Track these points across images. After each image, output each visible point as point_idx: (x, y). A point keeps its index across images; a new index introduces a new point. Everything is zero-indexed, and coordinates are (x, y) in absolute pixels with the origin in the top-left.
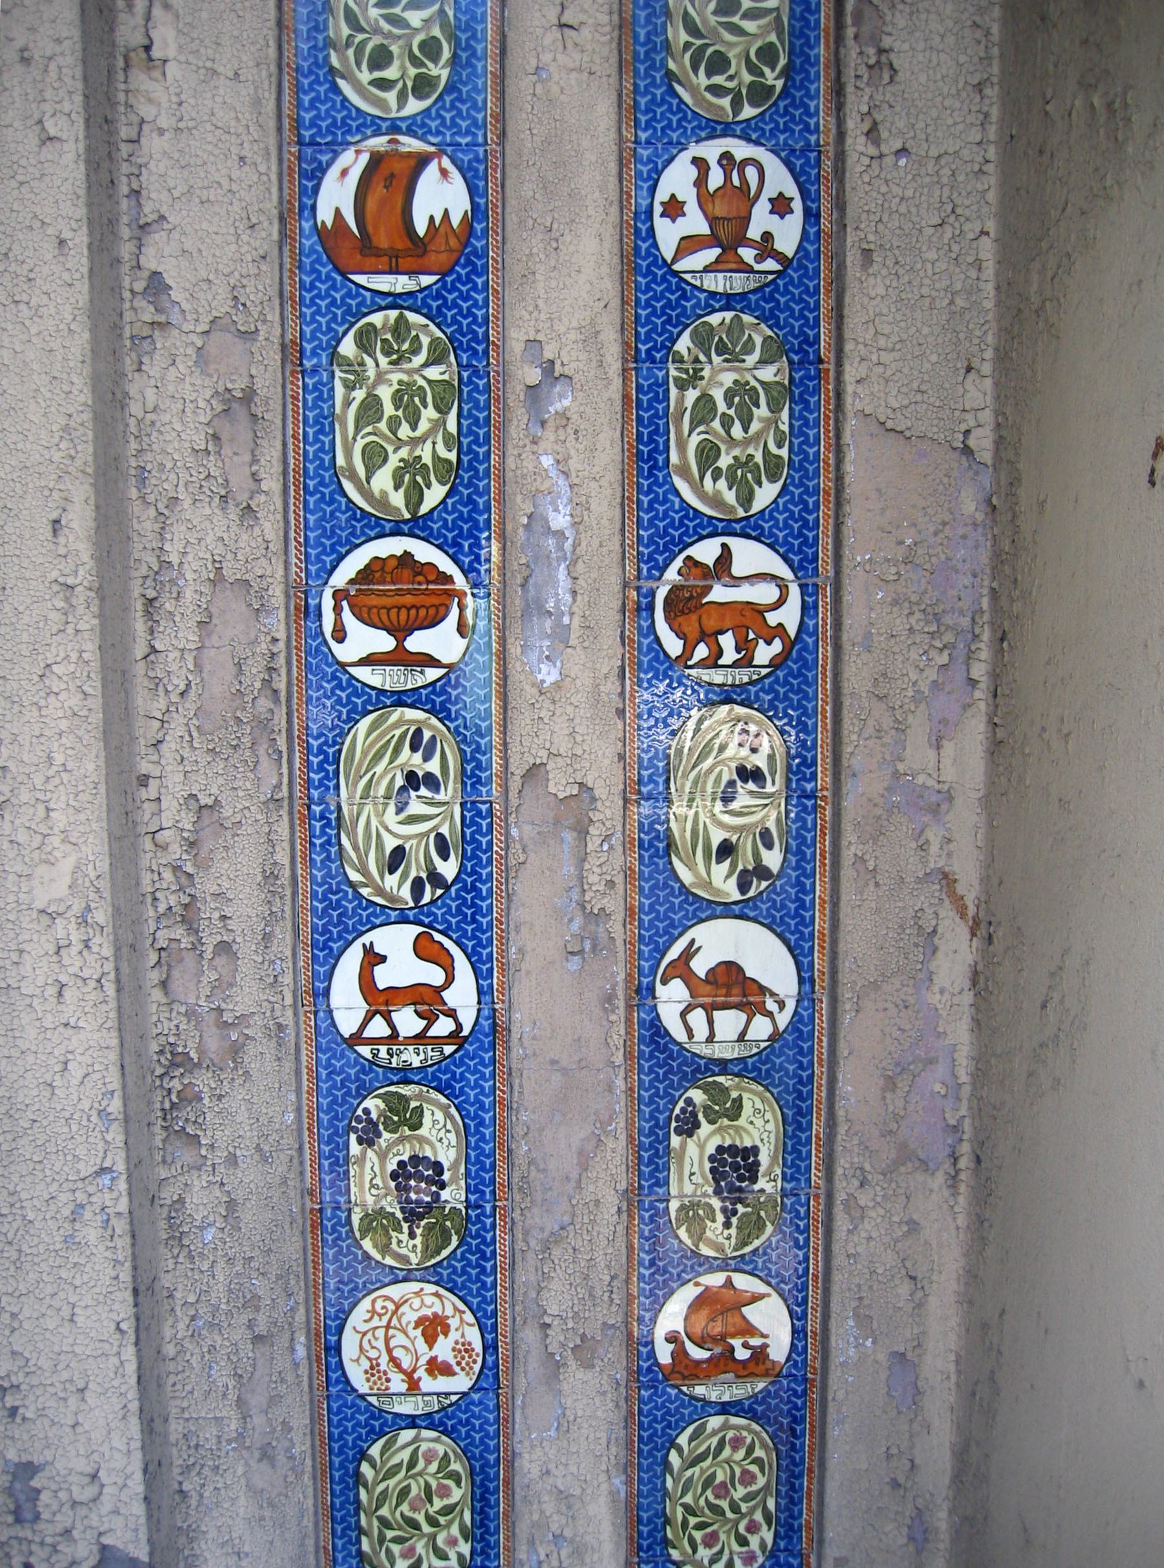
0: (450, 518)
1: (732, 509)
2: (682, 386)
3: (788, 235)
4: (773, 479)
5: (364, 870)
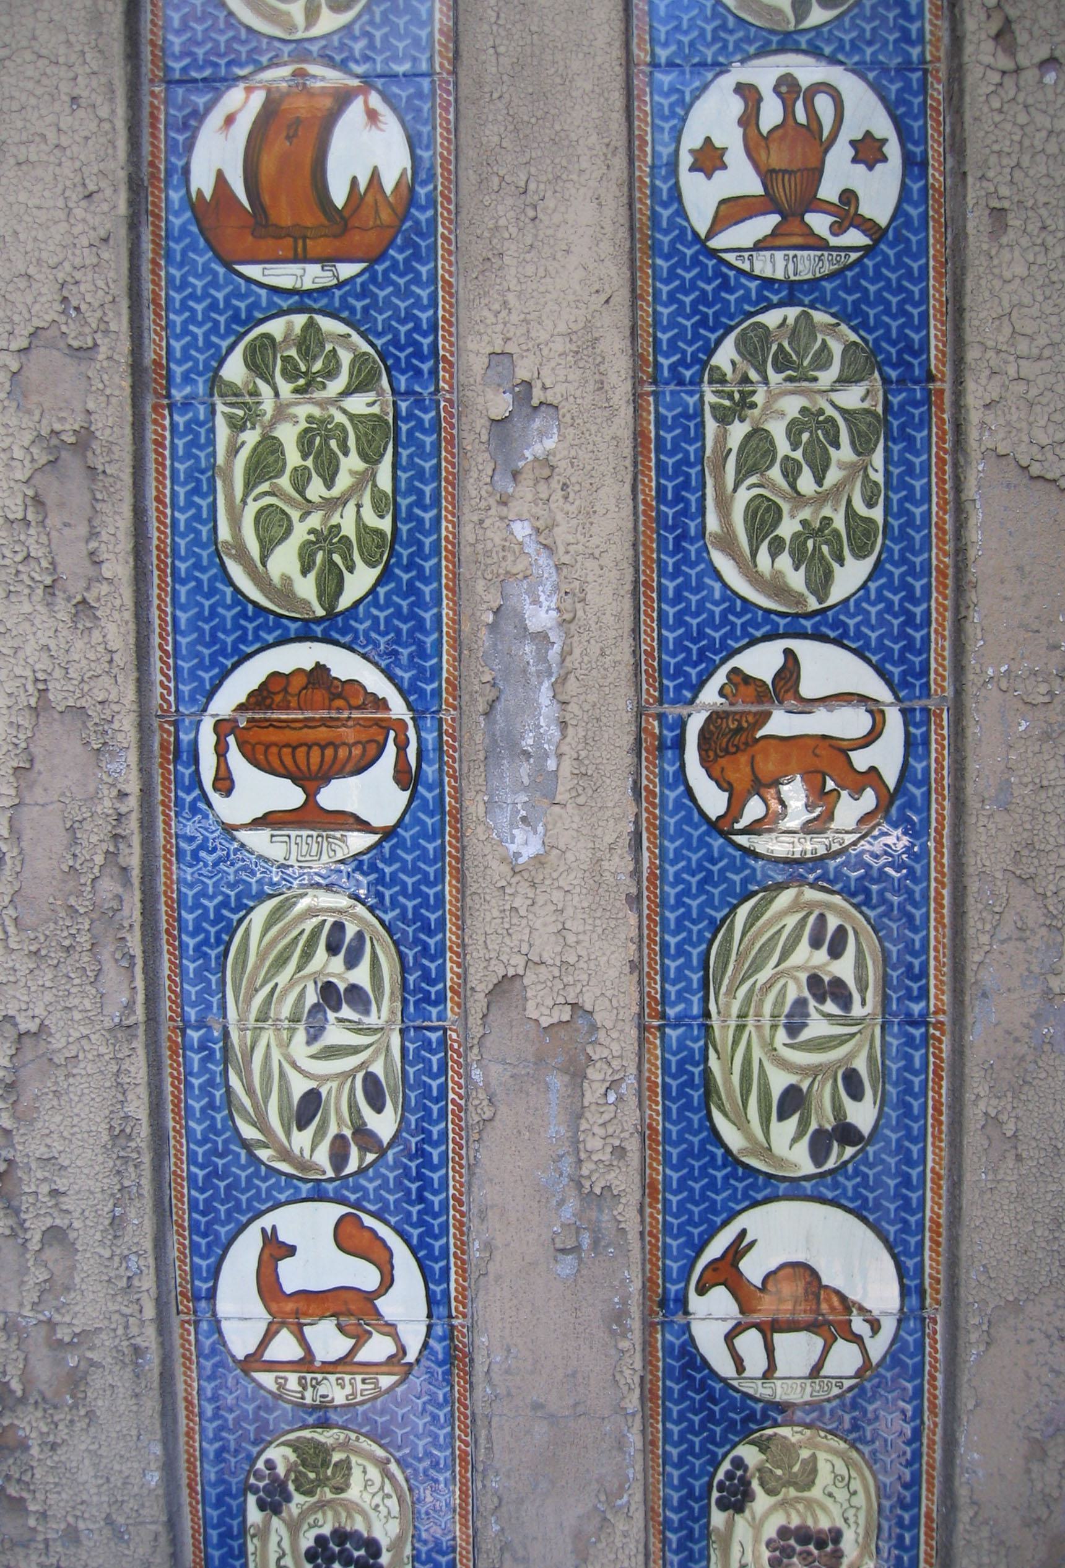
0: (382, 615)
1: (800, 599)
2: (724, 417)
3: (879, 193)
4: (860, 553)
5: (261, 1123)
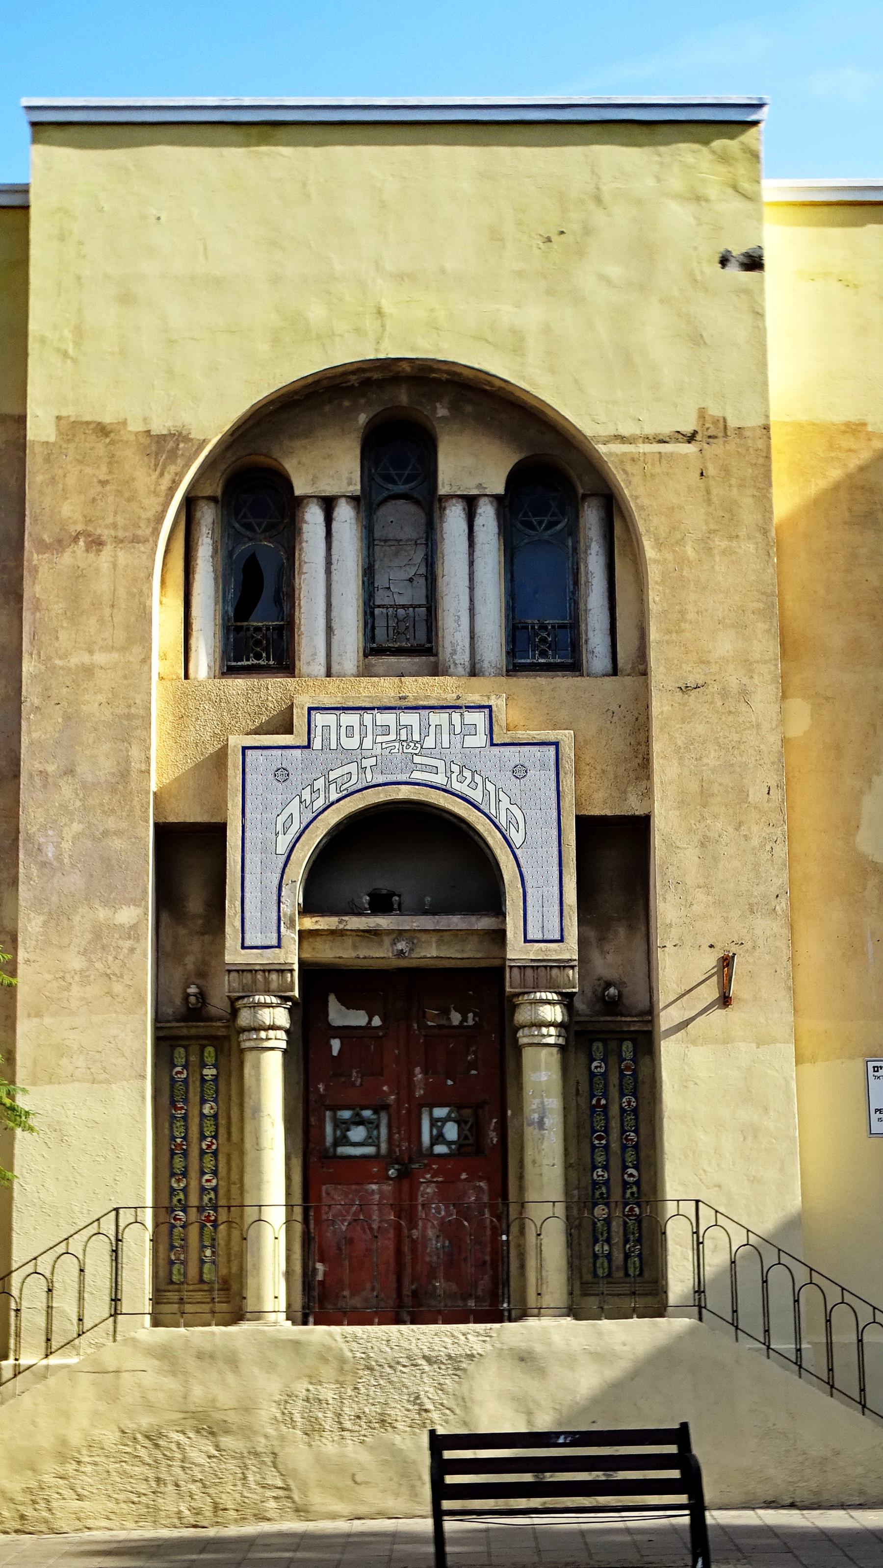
3: (634, 1104)
